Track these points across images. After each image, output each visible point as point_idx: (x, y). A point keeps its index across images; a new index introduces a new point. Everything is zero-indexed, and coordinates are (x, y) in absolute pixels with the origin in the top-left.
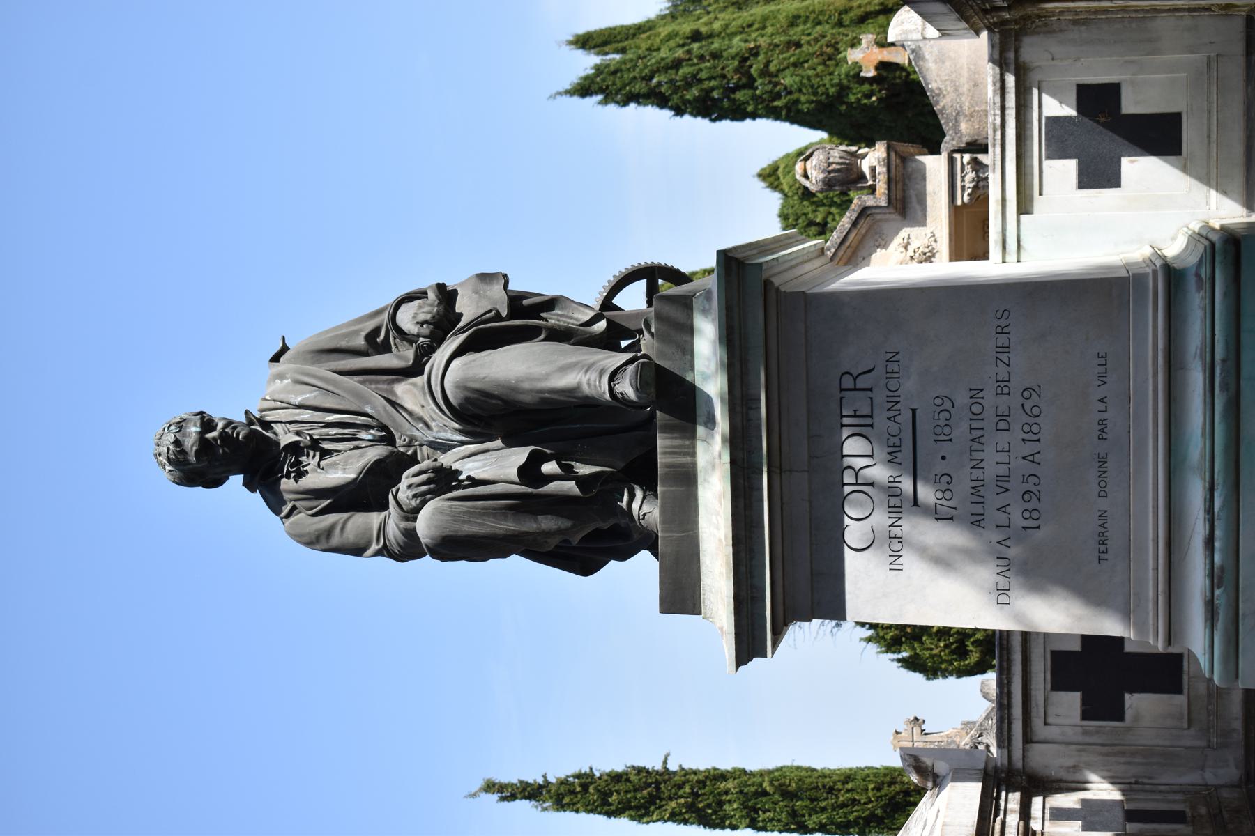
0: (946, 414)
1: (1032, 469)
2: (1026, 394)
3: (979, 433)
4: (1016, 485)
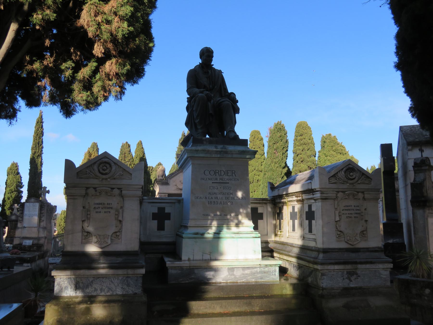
1: (219, 203)
4: (216, 200)
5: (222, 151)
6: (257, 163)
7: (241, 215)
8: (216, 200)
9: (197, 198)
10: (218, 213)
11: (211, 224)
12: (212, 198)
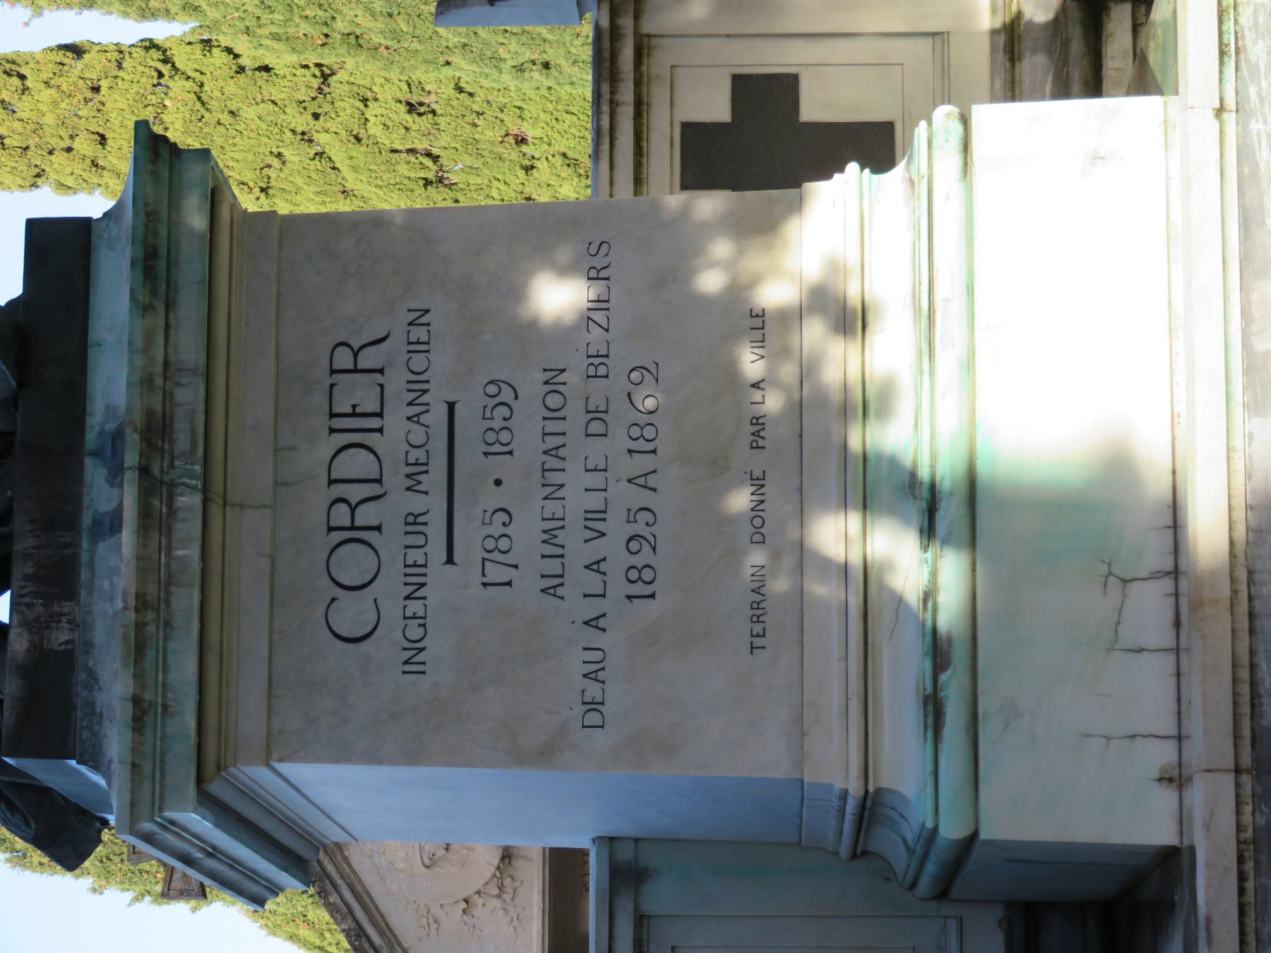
0: (504, 411)
1: (645, 498)
2: (635, 376)
3: (558, 441)
4: (617, 528)
5: (144, 471)
6: (249, 113)
7: (754, 282)
8: (617, 528)
9: (593, 706)
10: (740, 500)
11: (845, 569)
12: (594, 566)
